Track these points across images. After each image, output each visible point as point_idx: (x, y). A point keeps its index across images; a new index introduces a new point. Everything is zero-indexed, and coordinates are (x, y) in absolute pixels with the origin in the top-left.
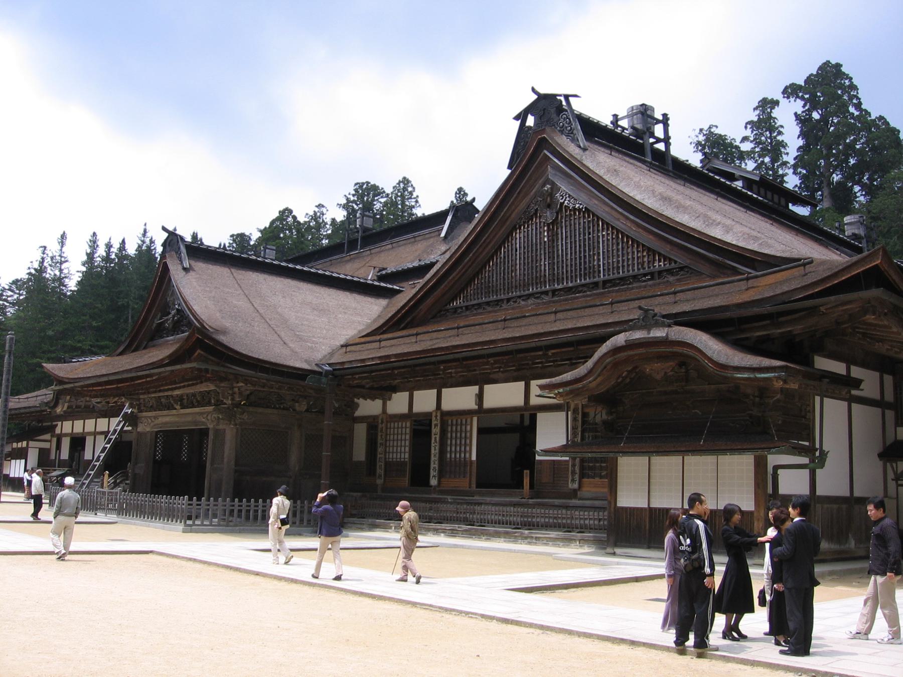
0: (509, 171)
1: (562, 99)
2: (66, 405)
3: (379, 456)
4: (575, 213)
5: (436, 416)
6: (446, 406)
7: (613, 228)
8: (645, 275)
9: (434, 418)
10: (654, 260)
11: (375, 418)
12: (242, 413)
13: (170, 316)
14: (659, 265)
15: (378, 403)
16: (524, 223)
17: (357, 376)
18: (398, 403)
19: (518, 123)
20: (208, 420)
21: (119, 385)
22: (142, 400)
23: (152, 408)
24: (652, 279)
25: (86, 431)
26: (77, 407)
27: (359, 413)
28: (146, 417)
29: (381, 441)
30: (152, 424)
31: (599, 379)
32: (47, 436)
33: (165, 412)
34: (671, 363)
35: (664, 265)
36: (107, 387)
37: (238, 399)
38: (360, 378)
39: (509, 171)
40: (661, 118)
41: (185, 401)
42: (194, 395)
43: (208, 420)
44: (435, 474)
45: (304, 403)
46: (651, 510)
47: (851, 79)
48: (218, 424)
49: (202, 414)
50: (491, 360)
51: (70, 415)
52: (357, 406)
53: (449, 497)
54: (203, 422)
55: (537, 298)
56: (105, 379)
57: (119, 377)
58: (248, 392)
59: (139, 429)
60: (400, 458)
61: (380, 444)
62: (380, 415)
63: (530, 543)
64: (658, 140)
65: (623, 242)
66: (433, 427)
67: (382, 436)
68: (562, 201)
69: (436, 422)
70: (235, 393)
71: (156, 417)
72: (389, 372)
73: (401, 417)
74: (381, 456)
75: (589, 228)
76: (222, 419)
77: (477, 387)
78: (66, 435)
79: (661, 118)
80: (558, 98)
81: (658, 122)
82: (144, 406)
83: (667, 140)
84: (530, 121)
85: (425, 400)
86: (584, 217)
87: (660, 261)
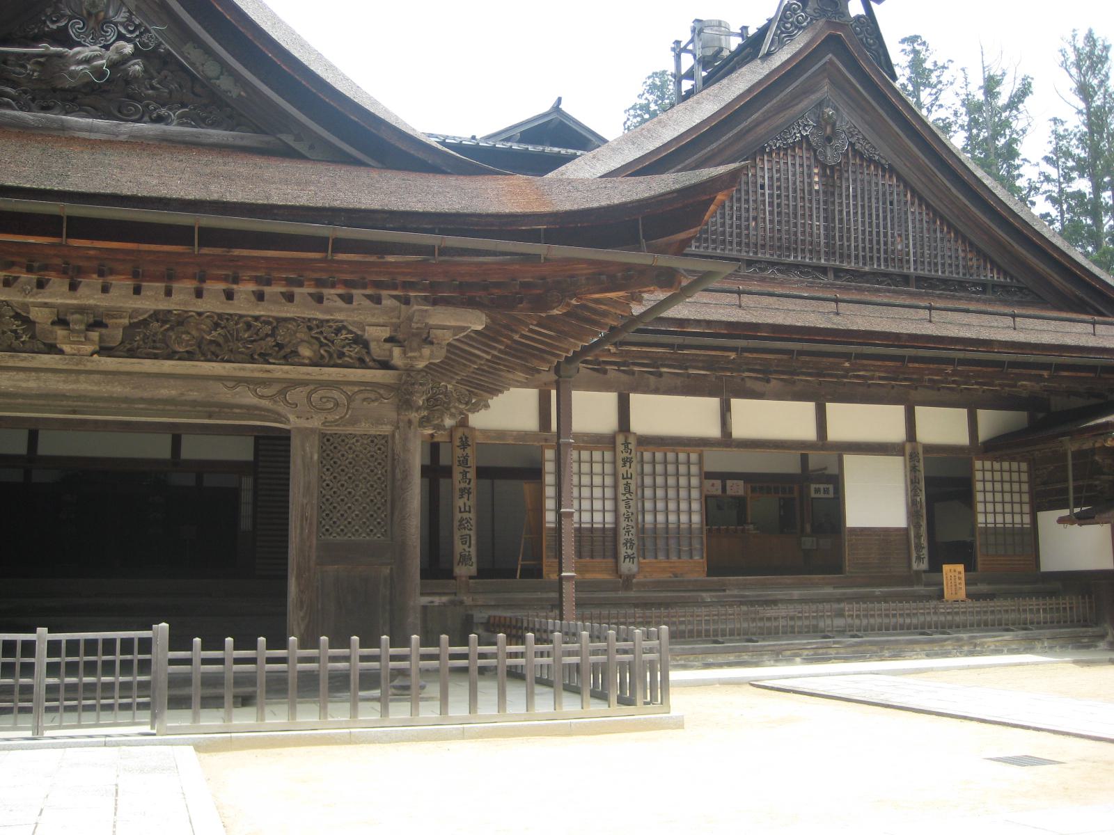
3: (458, 516)
4: (868, 167)
8: (975, 284)
14: (992, 276)
24: (984, 292)
29: (463, 485)
44: (630, 552)
53: (704, 594)
61: (462, 491)
67: (465, 473)
74: (465, 515)
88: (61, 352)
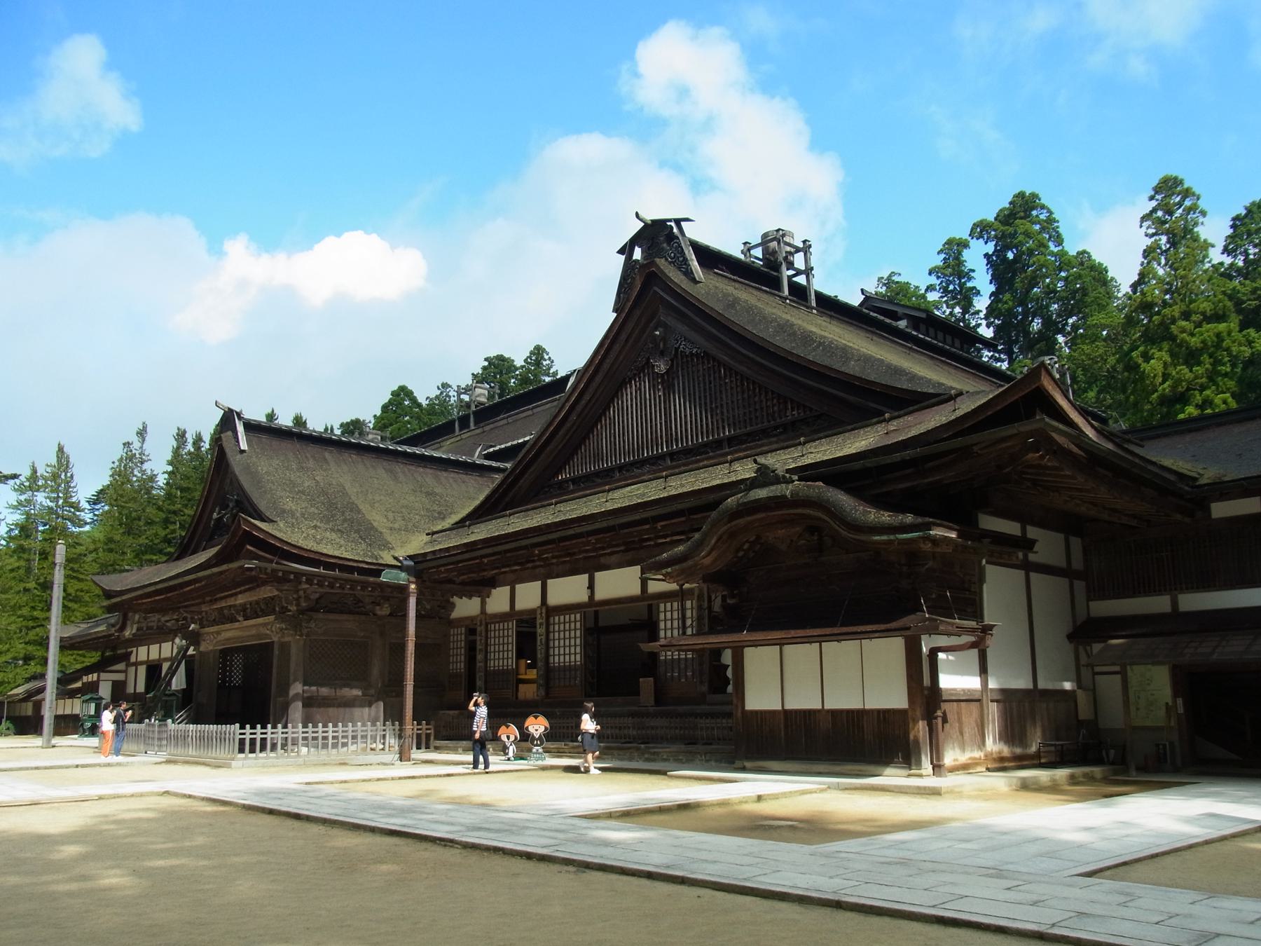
0: (615, 315)
1: (673, 224)
2: (135, 626)
3: (478, 664)
4: (692, 360)
5: (541, 613)
6: (553, 600)
7: (736, 373)
8: (776, 428)
9: (539, 616)
10: (786, 409)
11: (472, 619)
12: (309, 621)
13: (229, 509)
14: (792, 414)
15: (476, 601)
16: (635, 375)
17: (443, 569)
18: (498, 601)
19: (622, 258)
20: (272, 631)
21: (169, 595)
22: (204, 613)
23: (215, 623)
25: (162, 657)
26: (148, 628)
27: (456, 614)
28: (208, 633)
30: (214, 642)
31: (714, 554)
32: (121, 666)
33: (228, 626)
34: (798, 529)
35: (799, 414)
36: (157, 598)
37: (304, 604)
38: (447, 571)
39: (615, 315)
40: (801, 245)
41: (249, 610)
42: (257, 603)
43: (272, 631)
45: (386, 606)
46: (787, 714)
47: (1051, 213)
48: (282, 637)
49: (265, 625)
50: (592, 539)
51: (138, 640)
52: (453, 605)
54: (267, 635)
55: (653, 464)
56: (152, 589)
57: (166, 585)
58: (317, 595)
59: (202, 649)
60: (499, 666)
61: (480, 650)
62: (478, 616)
63: (648, 760)
64: (799, 272)
65: (749, 390)
66: (538, 626)
67: (481, 640)
68: (677, 346)
69: (541, 621)
70: (300, 597)
71: (218, 633)
72: (477, 561)
73: (503, 617)
74: (481, 664)
75: (710, 376)
76: (286, 629)
77: (587, 575)
78: (142, 663)
79: (801, 245)
80: (668, 223)
81: (798, 250)
82: (207, 620)
83: (808, 271)
84: (638, 254)
85: (528, 595)
86: (703, 363)
87: (793, 410)
88: (239, 621)
